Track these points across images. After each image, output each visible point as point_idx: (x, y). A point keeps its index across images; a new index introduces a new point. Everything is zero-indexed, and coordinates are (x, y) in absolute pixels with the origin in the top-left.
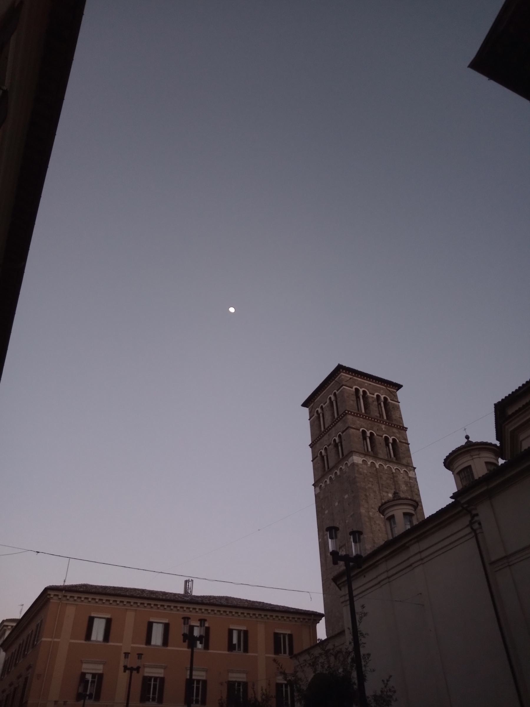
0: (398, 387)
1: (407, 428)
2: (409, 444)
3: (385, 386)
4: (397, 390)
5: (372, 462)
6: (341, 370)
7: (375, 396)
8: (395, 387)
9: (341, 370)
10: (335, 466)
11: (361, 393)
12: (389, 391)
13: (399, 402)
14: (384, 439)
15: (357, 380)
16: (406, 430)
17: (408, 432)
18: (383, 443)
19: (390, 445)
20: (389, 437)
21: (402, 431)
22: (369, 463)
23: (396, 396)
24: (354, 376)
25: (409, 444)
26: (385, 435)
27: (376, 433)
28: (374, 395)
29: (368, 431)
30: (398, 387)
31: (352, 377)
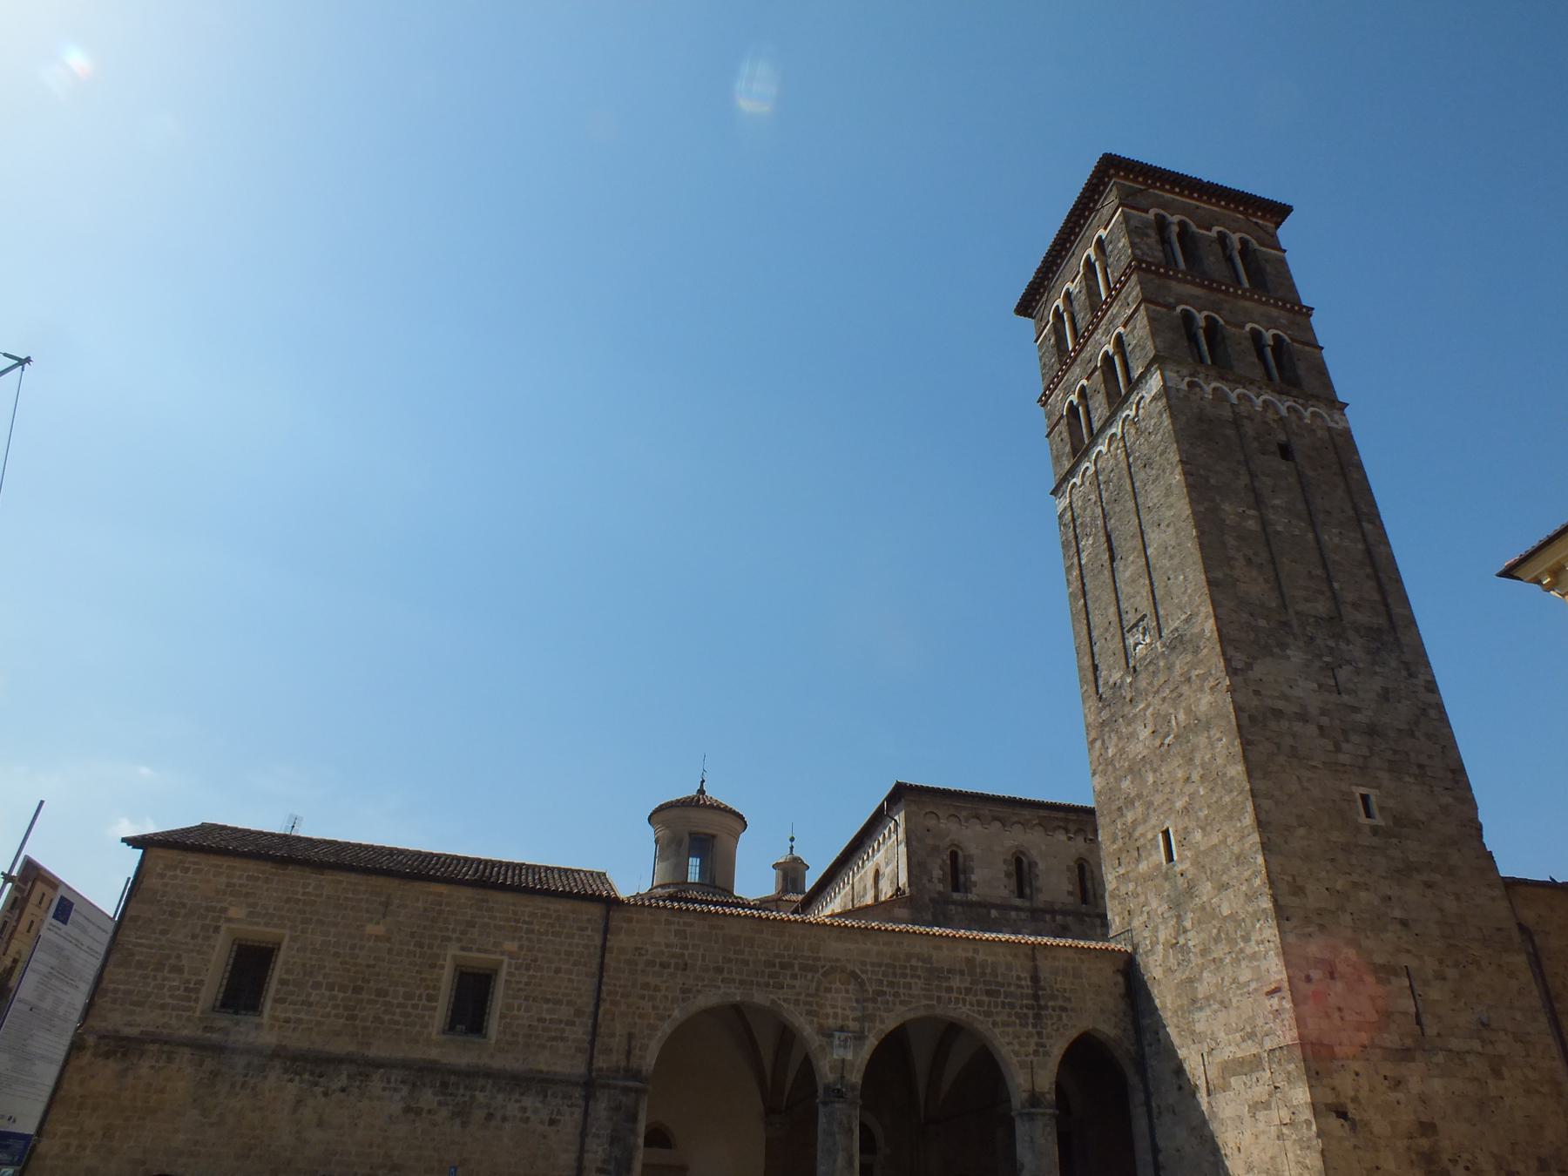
0: (1280, 212)
1: (1313, 309)
2: (1322, 348)
3: (1240, 212)
4: (1278, 225)
5: (1215, 389)
7: (1213, 233)
8: (1272, 217)
10: (1109, 422)
11: (1175, 229)
13: (1285, 251)
14: (1248, 335)
15: (1163, 197)
16: (1311, 315)
19: (1268, 350)
20: (1263, 330)
22: (1209, 389)
23: (1274, 236)
24: (1150, 186)
25: (1322, 348)
27: (1222, 318)
28: (1209, 229)
29: (1200, 311)
30: (1280, 212)
31: (1143, 187)
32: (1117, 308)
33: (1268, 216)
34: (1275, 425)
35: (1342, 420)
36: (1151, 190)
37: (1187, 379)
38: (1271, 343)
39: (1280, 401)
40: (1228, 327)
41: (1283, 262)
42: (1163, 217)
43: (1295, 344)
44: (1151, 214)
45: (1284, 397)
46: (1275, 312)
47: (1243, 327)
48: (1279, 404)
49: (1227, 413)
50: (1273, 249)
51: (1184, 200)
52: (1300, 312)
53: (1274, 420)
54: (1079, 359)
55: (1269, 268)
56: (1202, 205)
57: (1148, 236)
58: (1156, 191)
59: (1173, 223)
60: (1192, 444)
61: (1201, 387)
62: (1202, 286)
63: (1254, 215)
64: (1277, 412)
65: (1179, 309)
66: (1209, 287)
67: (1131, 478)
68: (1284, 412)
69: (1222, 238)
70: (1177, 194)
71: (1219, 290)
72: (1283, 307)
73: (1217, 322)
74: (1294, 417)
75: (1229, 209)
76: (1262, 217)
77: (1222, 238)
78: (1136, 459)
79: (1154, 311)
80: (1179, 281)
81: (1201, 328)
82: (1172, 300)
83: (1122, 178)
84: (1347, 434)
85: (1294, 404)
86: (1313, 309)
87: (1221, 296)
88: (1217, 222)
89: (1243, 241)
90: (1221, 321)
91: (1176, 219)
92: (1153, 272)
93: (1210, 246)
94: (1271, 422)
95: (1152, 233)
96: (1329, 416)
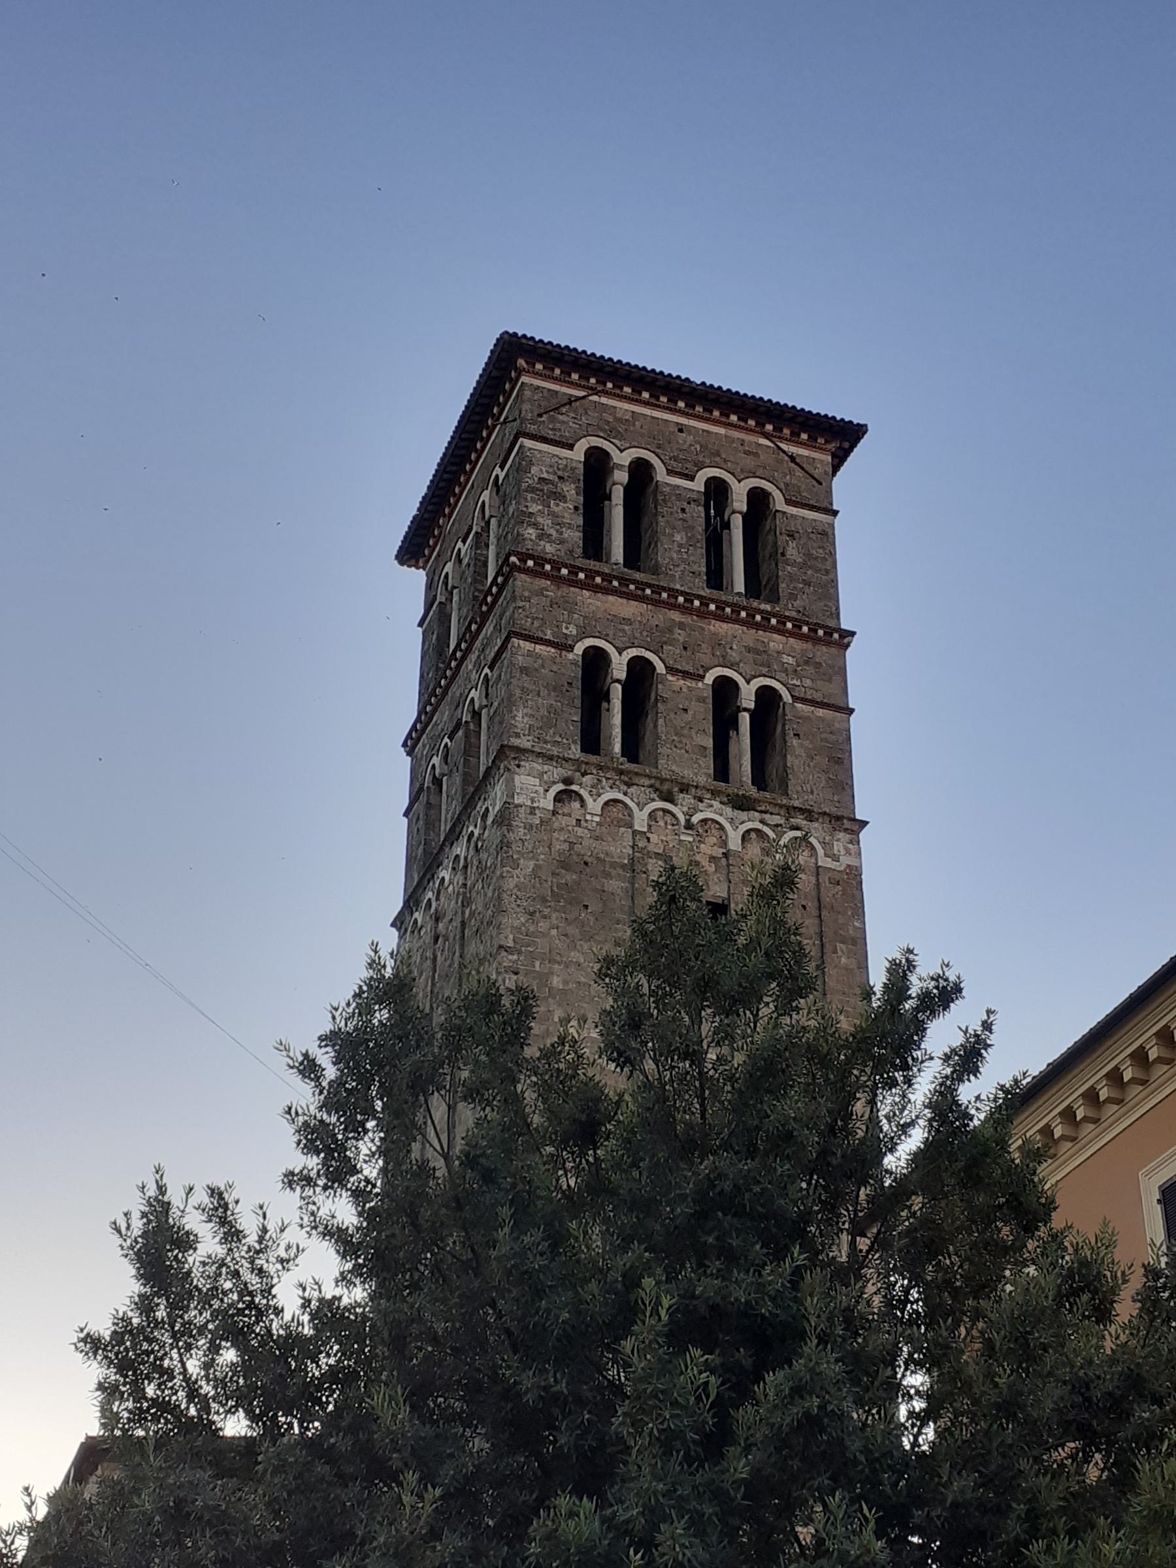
1: (853, 634)
3: (766, 436)
4: (839, 459)
6: (521, 362)
7: (698, 485)
8: (827, 442)
9: (521, 362)
12: (792, 458)
14: (708, 693)
16: (848, 645)
17: (851, 655)
18: (703, 713)
21: (823, 653)
22: (594, 806)
23: (823, 484)
25: (852, 711)
26: (719, 671)
28: (691, 478)
31: (582, 393)
32: (492, 628)
33: (821, 440)
34: (711, 868)
35: (848, 852)
36: (595, 398)
37: (561, 787)
38: (752, 706)
39: (731, 821)
40: (670, 678)
41: (826, 536)
42: (607, 454)
43: (799, 705)
44: (578, 454)
45: (743, 815)
46: (776, 642)
47: (702, 677)
48: (727, 826)
49: (620, 848)
50: (812, 508)
51: (657, 414)
52: (829, 643)
53: (713, 859)
54: (448, 698)
55: (792, 551)
56: (693, 423)
57: (561, 497)
58: (604, 400)
59: (620, 467)
60: (532, 914)
61: (582, 801)
62: (642, 599)
63: (794, 439)
64: (724, 843)
65: (579, 648)
66: (657, 603)
67: (462, 946)
68: (734, 843)
69: (717, 491)
70: (646, 403)
71: (675, 607)
72: (796, 634)
73: (654, 668)
74: (754, 850)
75: (749, 430)
76: (811, 444)
77: (717, 491)
78: (472, 914)
79: (530, 654)
80: (596, 589)
81: (618, 681)
82: (573, 630)
83: (537, 374)
84: (852, 880)
85: (760, 826)
86: (853, 634)
87: (676, 616)
88: (714, 456)
89: (758, 498)
90: (660, 668)
91: (623, 458)
92: (546, 576)
93: (683, 510)
94: (705, 862)
95: (570, 490)
96: (823, 843)
